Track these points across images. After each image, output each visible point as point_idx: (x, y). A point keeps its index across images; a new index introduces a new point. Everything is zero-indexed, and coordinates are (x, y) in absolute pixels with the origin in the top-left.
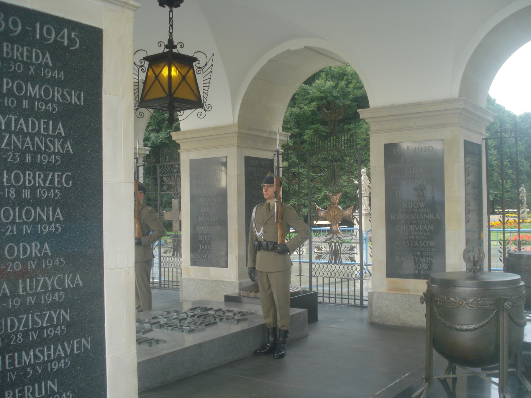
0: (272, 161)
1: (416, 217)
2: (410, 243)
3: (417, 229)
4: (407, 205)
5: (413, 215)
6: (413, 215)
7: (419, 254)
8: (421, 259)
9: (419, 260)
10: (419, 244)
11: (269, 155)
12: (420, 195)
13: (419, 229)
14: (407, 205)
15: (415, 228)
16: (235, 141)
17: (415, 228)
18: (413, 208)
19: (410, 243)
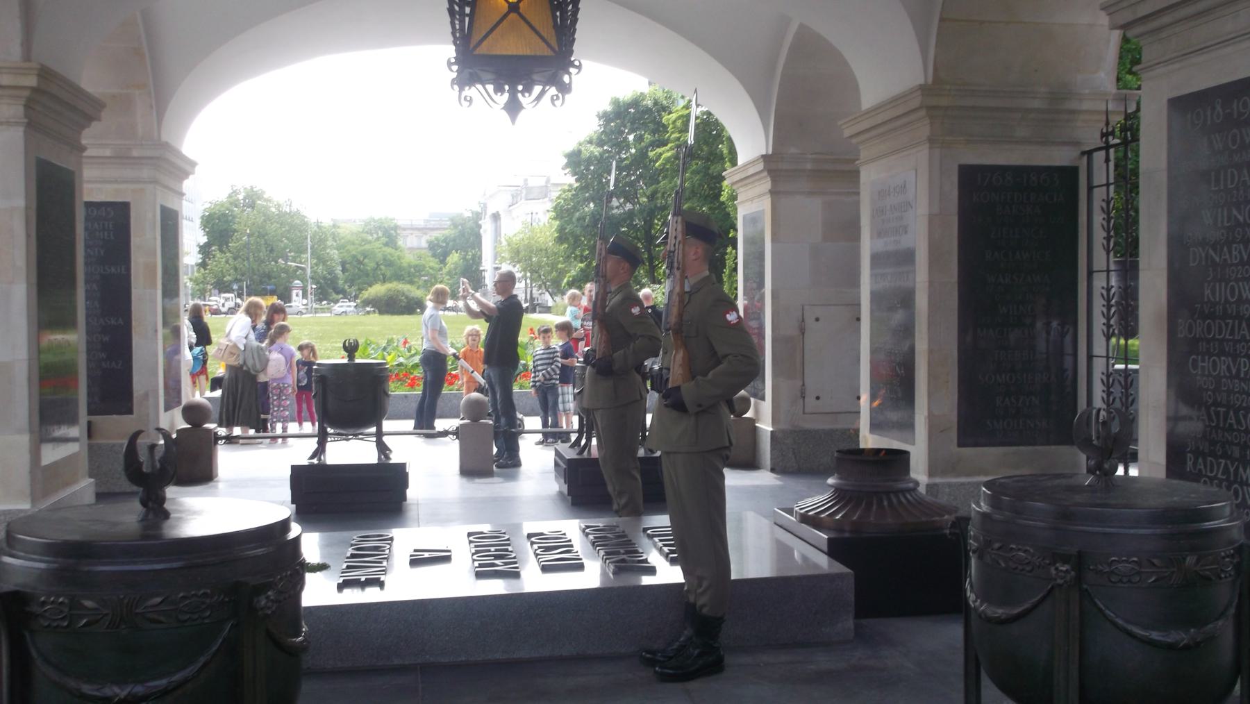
0: (1069, 174)
1: (1232, 333)
2: (1217, 414)
3: (1234, 371)
4: (1213, 292)
5: (1227, 325)
6: (1227, 325)
7: (1236, 452)
8: (1241, 469)
9: (1237, 470)
10: (1239, 422)
11: (1060, 157)
12: (1242, 258)
13: (1239, 370)
14: (1213, 292)
15: (1228, 367)
16: (924, 130)
17: (1228, 367)
18: (1227, 301)
19: (1217, 414)
